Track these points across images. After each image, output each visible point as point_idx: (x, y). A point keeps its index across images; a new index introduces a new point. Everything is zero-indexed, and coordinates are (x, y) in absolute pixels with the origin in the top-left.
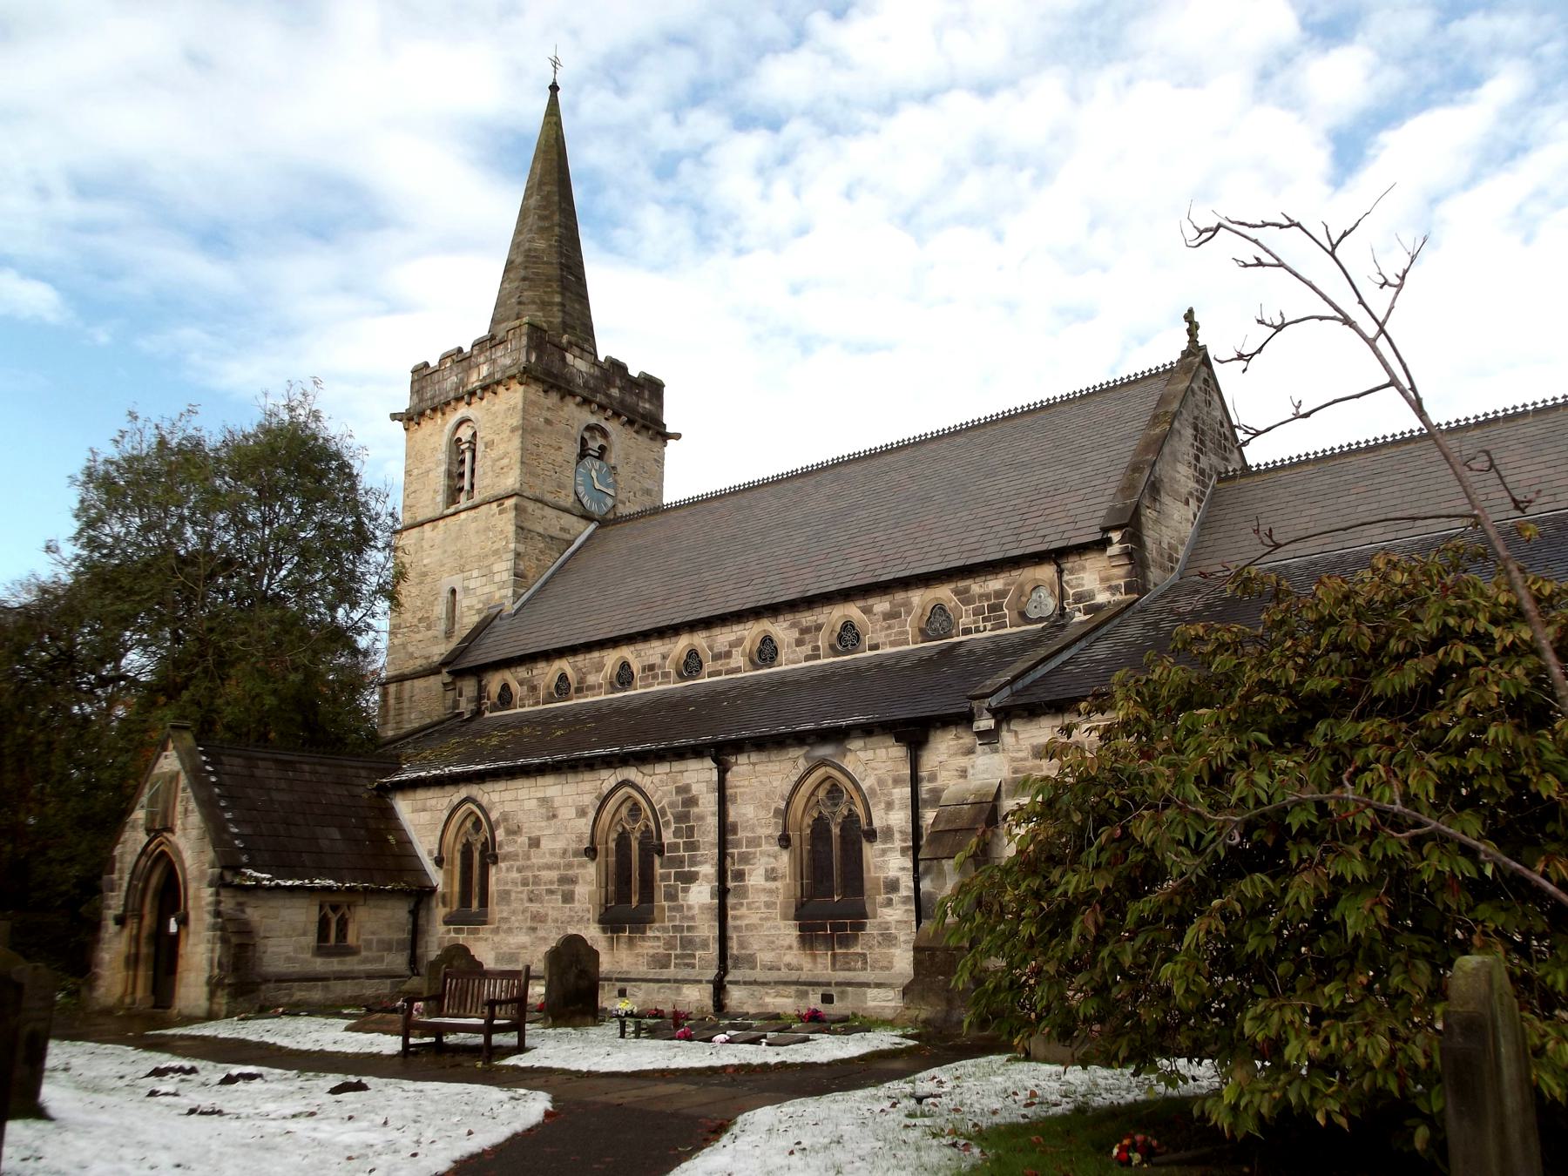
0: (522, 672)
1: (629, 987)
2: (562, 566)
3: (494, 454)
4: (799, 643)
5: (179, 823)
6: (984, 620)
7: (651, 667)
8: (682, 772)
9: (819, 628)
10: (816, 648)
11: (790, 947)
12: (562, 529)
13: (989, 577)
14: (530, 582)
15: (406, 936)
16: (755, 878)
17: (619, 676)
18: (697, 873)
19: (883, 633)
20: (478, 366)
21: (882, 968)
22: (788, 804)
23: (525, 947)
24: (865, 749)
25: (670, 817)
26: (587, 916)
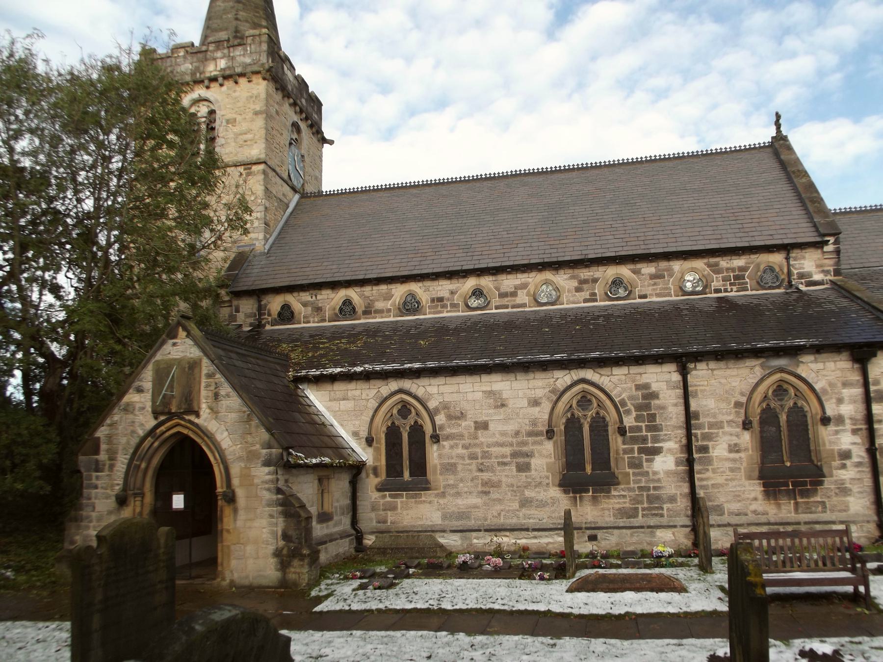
0: (306, 296)
1: (600, 534)
2: (286, 222)
3: (236, 130)
4: (578, 290)
5: (204, 406)
6: (731, 284)
7: (440, 300)
8: (641, 374)
9: (595, 281)
10: (594, 294)
11: (755, 499)
12: (284, 195)
13: (733, 258)
14: (272, 230)
15: (347, 502)
16: (719, 450)
17: (405, 303)
18: (662, 448)
19: (650, 288)
20: (215, 59)
21: (840, 511)
22: (750, 399)
23: (478, 507)
24: (816, 361)
25: (630, 406)
26: (545, 481)
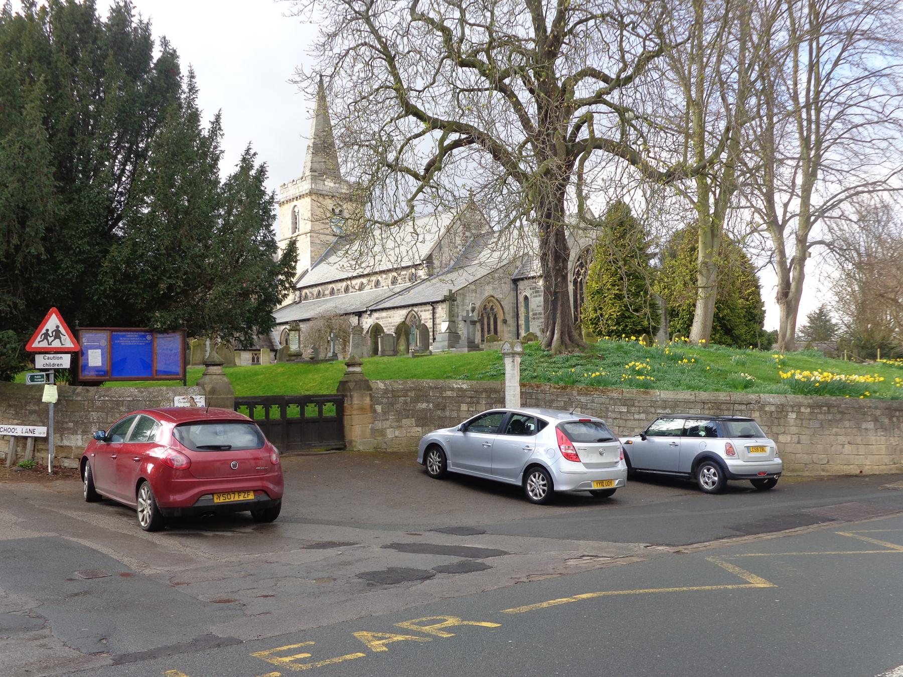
0: (310, 290)
7: (339, 290)
